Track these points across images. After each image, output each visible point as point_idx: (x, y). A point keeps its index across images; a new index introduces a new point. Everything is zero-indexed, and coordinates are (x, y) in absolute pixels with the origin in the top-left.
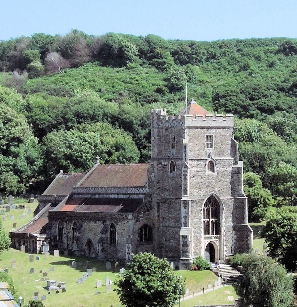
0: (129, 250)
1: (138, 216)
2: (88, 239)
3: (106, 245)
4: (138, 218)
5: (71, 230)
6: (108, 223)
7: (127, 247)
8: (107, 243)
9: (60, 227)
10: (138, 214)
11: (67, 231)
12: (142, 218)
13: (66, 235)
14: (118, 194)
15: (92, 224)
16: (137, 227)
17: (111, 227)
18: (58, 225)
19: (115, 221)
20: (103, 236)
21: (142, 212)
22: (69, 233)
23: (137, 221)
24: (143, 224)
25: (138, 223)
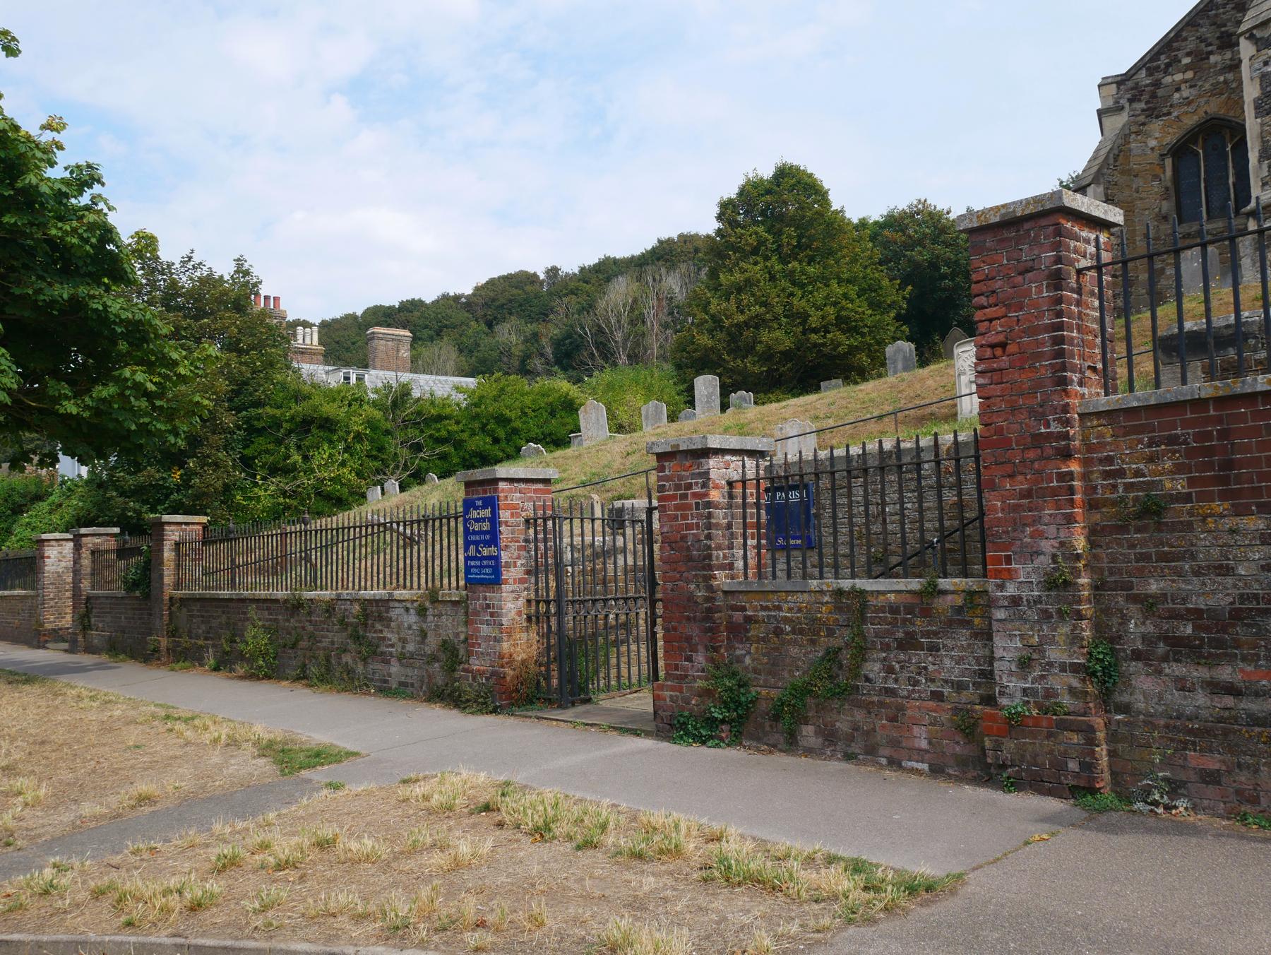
1: (1157, 84)
4: (1154, 96)
10: (1160, 75)
12: (1186, 92)
16: (1153, 143)
21: (1186, 60)
23: (1152, 113)
24: (1190, 121)
25: (1156, 126)
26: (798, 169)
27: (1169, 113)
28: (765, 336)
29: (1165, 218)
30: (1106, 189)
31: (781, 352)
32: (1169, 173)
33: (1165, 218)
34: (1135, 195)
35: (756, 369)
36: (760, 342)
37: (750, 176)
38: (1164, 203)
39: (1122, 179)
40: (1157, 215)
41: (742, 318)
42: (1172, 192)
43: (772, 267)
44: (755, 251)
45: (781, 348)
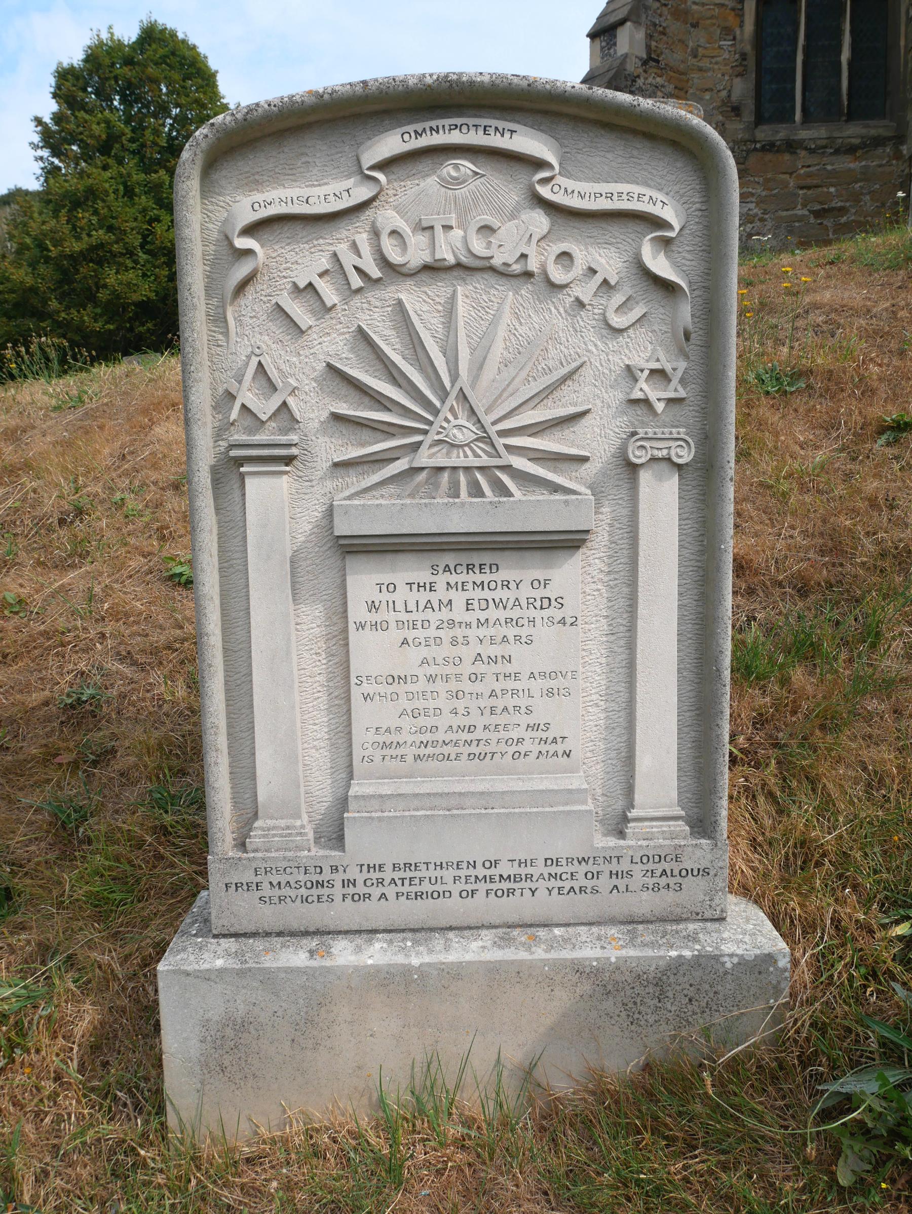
26: (173, 34)
28: (111, 277)
29: (736, 110)
30: (649, 37)
31: (135, 304)
32: (749, 26)
33: (736, 110)
34: (692, 61)
35: (98, 326)
36: (105, 286)
37: (105, 36)
38: (737, 81)
39: (675, 27)
40: (724, 103)
41: (77, 247)
42: (751, 63)
43: (129, 175)
44: (105, 148)
45: (136, 297)
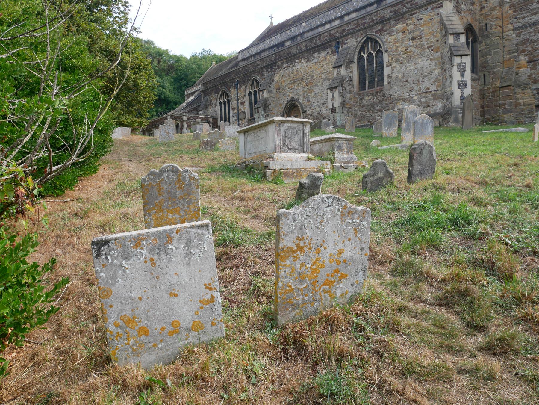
0: (462, 75)
2: (288, 102)
3: (349, 95)
5: (247, 99)
6: (353, 43)
7: (459, 65)
8: (350, 92)
9: (222, 101)
11: (238, 102)
13: (235, 111)
14: (342, 17)
15: (301, 66)
17: (362, 49)
18: (218, 100)
19: (379, 28)
20: (343, 71)
22: (243, 104)
27: (461, 13)
